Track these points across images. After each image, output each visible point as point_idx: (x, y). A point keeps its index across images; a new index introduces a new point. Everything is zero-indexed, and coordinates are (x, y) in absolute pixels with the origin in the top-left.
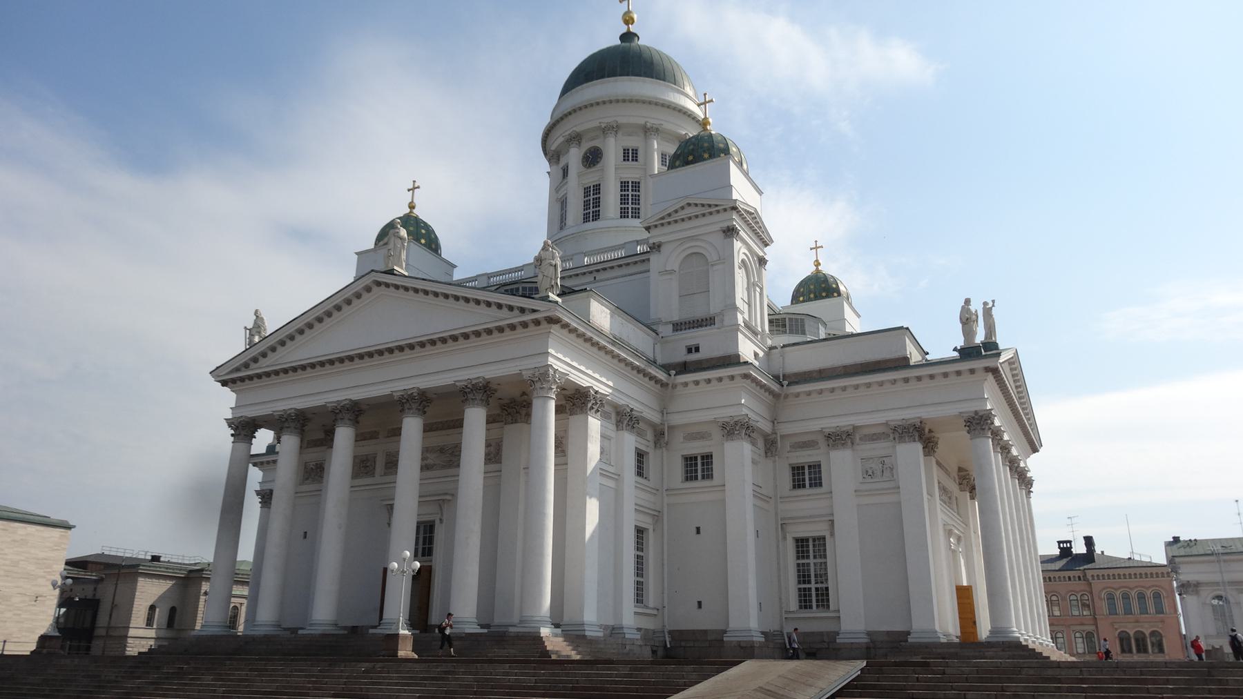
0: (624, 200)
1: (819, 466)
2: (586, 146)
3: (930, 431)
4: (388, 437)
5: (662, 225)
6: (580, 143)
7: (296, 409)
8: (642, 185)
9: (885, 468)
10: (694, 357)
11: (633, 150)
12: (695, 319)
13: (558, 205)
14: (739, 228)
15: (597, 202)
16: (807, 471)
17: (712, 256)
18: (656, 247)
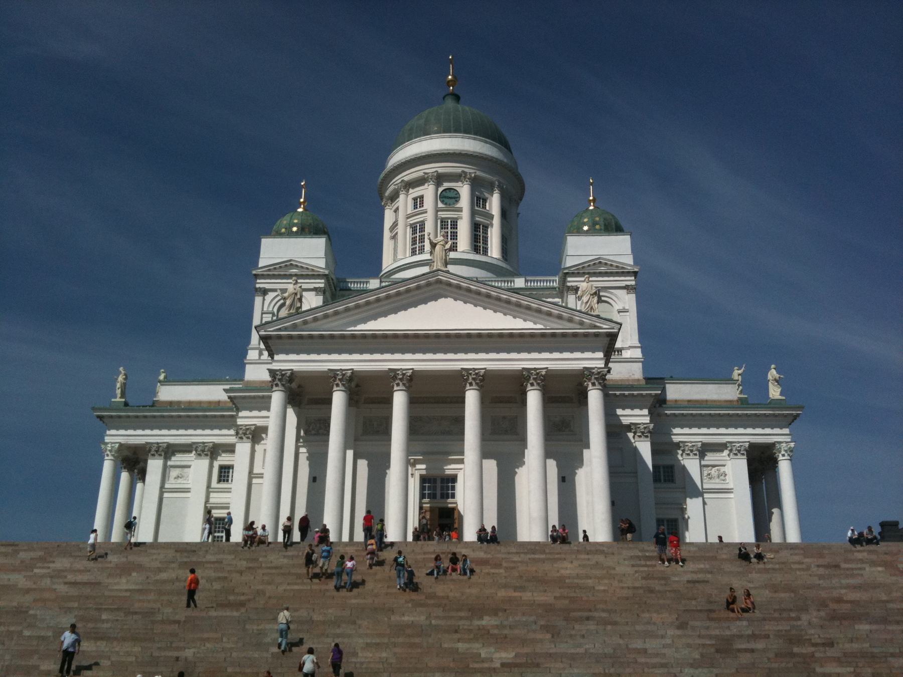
15: (454, 236)
16: (662, 470)
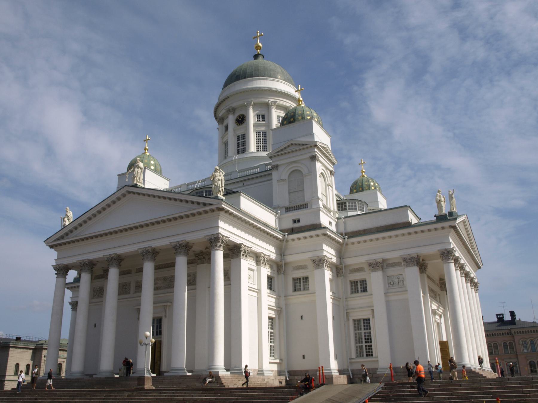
0: (258, 141)
1: (366, 281)
2: (238, 114)
3: (423, 260)
4: (136, 272)
5: (278, 155)
6: (234, 112)
7: (88, 259)
8: (267, 134)
9: (399, 281)
10: (297, 225)
11: (262, 115)
12: (297, 205)
13: (223, 146)
14: (319, 156)
15: (244, 144)
17: (305, 171)
18: (275, 167)
